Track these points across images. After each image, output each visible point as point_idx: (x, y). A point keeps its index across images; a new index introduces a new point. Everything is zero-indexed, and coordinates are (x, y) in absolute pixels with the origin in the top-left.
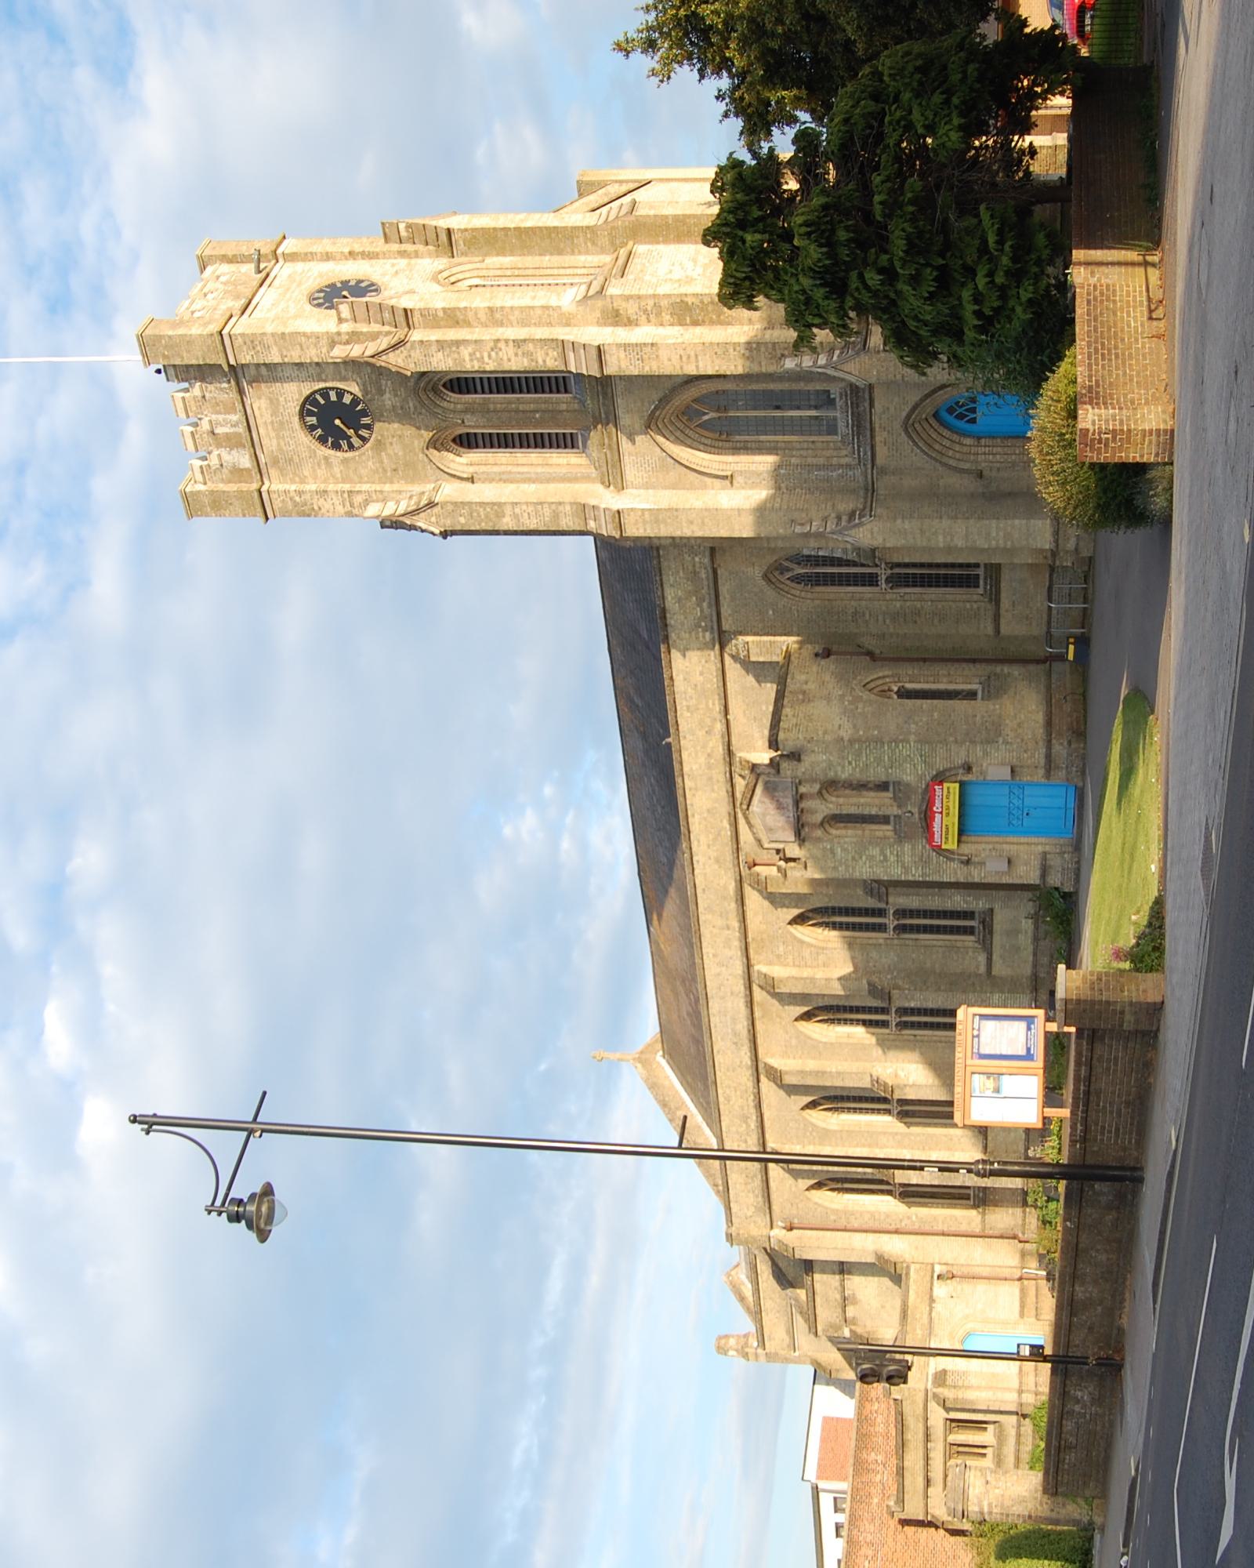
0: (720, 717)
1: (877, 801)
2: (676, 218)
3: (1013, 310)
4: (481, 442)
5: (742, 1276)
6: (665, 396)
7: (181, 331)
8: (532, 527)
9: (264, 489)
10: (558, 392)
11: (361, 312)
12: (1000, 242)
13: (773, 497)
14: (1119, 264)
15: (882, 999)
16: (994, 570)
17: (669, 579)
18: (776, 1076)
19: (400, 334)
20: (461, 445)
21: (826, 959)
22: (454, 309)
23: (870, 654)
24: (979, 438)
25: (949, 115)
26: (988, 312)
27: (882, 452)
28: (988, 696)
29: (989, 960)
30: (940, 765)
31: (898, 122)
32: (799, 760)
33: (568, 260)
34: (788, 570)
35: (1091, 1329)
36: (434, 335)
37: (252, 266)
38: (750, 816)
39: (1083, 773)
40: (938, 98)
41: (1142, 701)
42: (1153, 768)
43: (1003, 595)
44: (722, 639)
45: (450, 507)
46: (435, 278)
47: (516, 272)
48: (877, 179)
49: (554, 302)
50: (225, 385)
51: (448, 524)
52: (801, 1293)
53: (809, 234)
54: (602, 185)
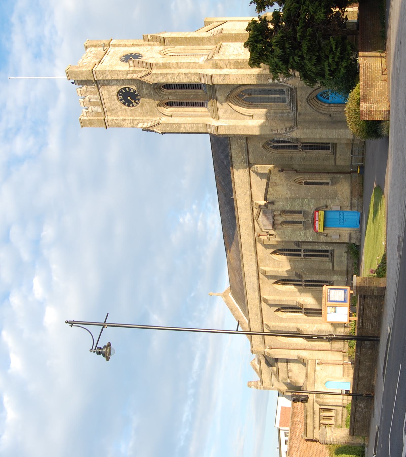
0: (249, 190)
1: (298, 217)
2: (235, 34)
3: (340, 69)
4: (174, 105)
5: (256, 363)
6: (232, 91)
7: (80, 69)
8: (190, 131)
9: (106, 119)
10: (198, 89)
11: (136, 64)
12: (336, 48)
13: (265, 122)
14: (373, 57)
15: (300, 277)
16: (335, 145)
17: (233, 147)
18: (266, 301)
19: (149, 71)
20: (168, 105)
21: (282, 265)
22: (165, 63)
23: (296, 171)
24: (330, 104)
25: (320, 9)
26: (333, 70)
27: (300, 108)
28: (333, 184)
29: (333, 265)
30: (318, 206)
31: (305, 10)
32: (274, 204)
33: (201, 47)
34: (270, 144)
36: (159, 71)
37: (102, 48)
38: (259, 222)
39: (362, 208)
40: (317, 3)
41: (380, 190)
42: (383, 212)
43: (337, 152)
44: (250, 166)
45: (164, 125)
46: (160, 53)
47: (185, 51)
48: (298, 28)
49: (197, 61)
50: (93, 86)
51: (164, 130)
52: (274, 368)
53: (277, 45)
54: (212, 22)
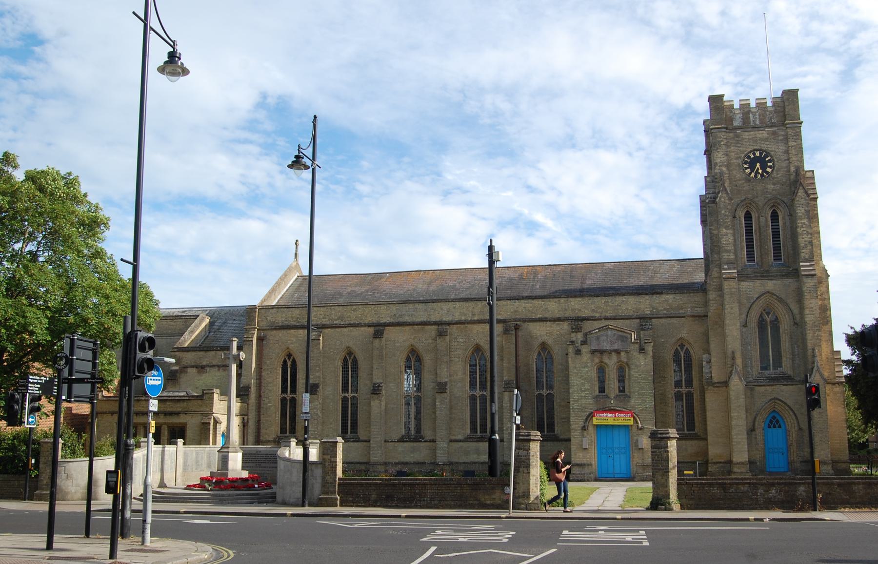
0: (603, 315)
17: (678, 297)
27: (762, 389)
29: (460, 441)
34: (682, 349)
35: (830, 494)
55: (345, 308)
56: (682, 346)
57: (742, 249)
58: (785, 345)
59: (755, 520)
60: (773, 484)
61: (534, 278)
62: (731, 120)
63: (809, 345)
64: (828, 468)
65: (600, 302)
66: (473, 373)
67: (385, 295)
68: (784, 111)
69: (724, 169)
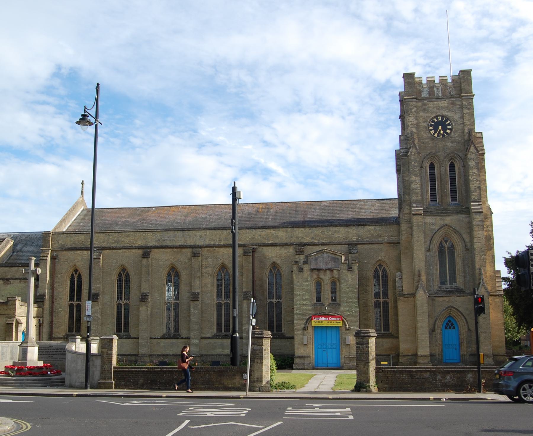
0: (320, 241)
17: (378, 228)
27: (441, 299)
29: (209, 338)
55: (120, 234)
56: (380, 266)
57: (427, 191)
58: (459, 266)
59: (435, 399)
60: (448, 372)
61: (267, 212)
62: (420, 92)
63: (477, 266)
64: (490, 360)
65: (318, 231)
66: (219, 286)
67: (152, 224)
68: (461, 86)
69: (414, 130)
